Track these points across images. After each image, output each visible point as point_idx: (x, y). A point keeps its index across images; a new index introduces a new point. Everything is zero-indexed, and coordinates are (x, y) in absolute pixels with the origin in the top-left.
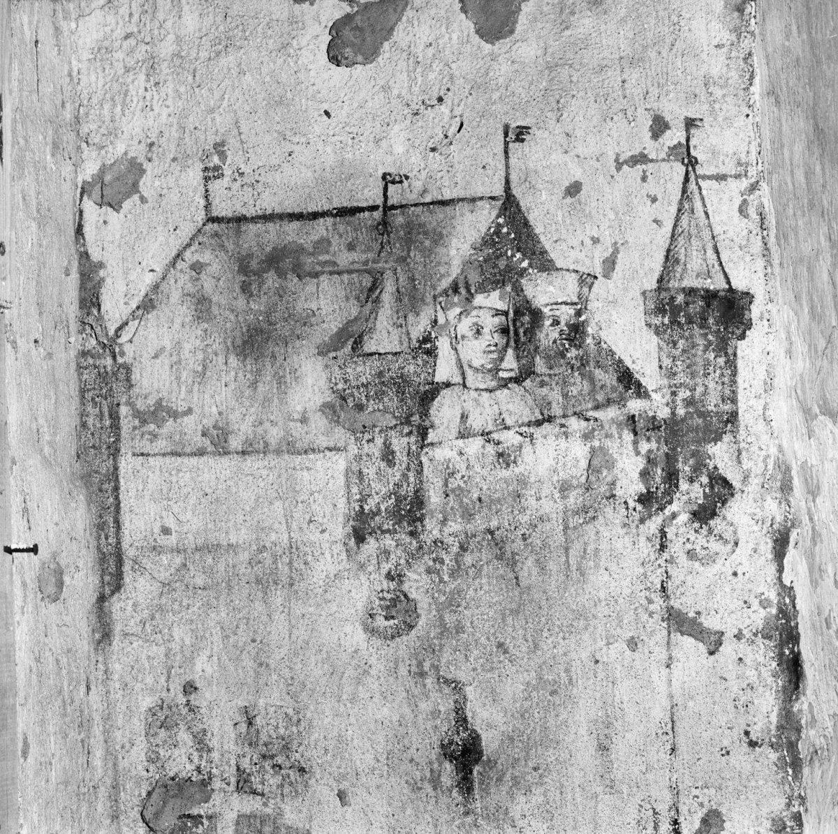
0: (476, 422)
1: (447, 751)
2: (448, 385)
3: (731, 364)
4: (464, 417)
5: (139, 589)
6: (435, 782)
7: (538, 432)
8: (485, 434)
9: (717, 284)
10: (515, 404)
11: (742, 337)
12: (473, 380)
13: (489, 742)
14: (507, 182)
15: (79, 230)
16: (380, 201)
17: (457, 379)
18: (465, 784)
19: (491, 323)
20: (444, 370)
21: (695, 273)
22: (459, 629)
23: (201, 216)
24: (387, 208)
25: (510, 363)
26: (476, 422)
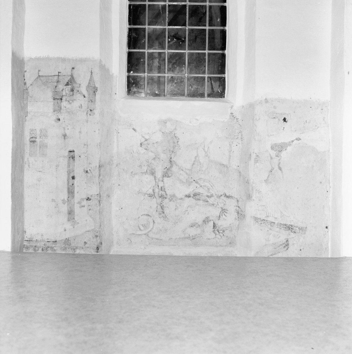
0: (67, 100)
2: (65, 95)
8: (68, 101)
13: (68, 134)
17: (66, 95)
18: (65, 138)
19: (69, 89)
23: (38, 76)
24: (59, 76)
26: (67, 100)
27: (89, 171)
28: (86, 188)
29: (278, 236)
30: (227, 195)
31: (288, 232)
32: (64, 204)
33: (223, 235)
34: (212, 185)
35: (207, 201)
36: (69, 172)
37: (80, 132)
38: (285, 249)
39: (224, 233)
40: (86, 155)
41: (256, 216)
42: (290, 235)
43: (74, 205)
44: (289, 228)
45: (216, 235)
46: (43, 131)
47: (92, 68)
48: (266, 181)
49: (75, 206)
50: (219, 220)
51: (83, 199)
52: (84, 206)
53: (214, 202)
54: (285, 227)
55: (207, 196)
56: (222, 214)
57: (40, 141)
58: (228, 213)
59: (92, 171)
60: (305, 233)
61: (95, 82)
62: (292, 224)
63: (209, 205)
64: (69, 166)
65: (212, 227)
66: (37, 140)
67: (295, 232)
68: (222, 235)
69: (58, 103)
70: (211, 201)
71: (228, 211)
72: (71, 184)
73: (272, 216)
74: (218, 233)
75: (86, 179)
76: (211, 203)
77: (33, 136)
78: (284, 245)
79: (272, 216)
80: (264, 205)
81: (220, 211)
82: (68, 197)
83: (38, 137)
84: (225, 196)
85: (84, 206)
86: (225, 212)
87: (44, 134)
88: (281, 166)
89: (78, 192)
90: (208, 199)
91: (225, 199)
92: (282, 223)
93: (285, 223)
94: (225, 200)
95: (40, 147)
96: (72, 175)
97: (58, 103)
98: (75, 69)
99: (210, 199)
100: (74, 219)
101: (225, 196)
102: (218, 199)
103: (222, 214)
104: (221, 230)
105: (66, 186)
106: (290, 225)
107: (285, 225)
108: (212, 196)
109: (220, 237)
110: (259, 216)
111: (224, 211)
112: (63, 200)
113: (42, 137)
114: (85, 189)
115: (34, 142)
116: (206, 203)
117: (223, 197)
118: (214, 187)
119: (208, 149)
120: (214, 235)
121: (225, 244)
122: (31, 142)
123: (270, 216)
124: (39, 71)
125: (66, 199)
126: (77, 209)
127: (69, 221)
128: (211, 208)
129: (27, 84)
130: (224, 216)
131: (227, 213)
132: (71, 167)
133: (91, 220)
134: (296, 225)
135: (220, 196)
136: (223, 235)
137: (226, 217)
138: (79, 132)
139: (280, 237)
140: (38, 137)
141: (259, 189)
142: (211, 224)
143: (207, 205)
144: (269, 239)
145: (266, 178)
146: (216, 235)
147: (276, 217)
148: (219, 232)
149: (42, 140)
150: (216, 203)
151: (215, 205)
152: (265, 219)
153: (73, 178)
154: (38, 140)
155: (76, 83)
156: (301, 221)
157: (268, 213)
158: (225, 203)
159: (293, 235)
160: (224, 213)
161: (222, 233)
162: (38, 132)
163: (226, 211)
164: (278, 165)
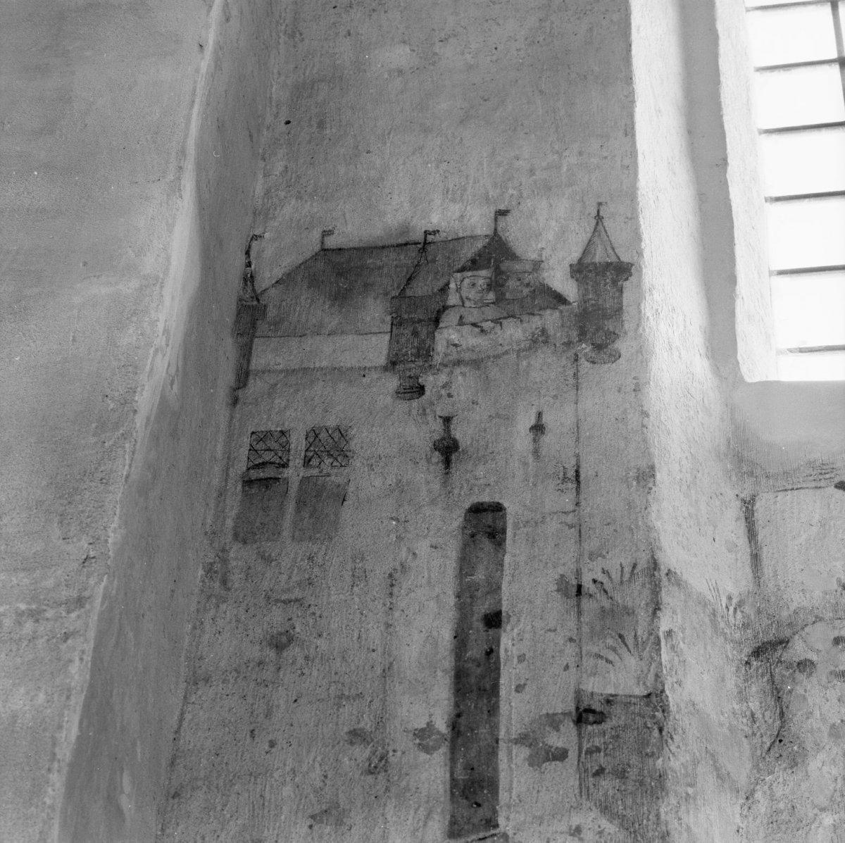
1: (436, 447)
3: (621, 291)
4: (461, 317)
5: (256, 386)
6: (429, 461)
7: (505, 322)
9: (613, 259)
10: (491, 312)
11: (627, 279)
12: (467, 304)
13: (462, 445)
14: (496, 229)
15: (248, 253)
16: (422, 240)
18: (447, 463)
19: (481, 282)
20: (453, 299)
21: (599, 256)
22: (450, 396)
25: (491, 296)
27: (586, 582)
28: (572, 665)
32: (427, 749)
36: (466, 595)
37: (538, 428)
40: (570, 519)
43: (493, 752)
46: (323, 435)
47: (600, 204)
49: (502, 755)
51: (553, 721)
52: (561, 755)
57: (305, 480)
59: (608, 586)
61: (615, 245)
64: (465, 565)
66: (288, 473)
69: (415, 334)
72: (475, 651)
75: (572, 624)
77: (267, 457)
82: (459, 716)
83: (296, 462)
85: (561, 755)
87: (331, 445)
89: (519, 688)
95: (301, 504)
96: (483, 607)
97: (415, 334)
98: (515, 213)
100: (491, 823)
105: (448, 663)
112: (423, 736)
113: (315, 462)
114: (567, 667)
115: (267, 482)
122: (248, 483)
124: (326, 233)
125: (442, 725)
126: (514, 773)
127: (459, 835)
129: (258, 279)
132: (480, 576)
133: (610, 828)
138: (532, 428)
140: (296, 462)
149: (315, 472)
153: (494, 620)
154: (294, 473)
155: (513, 257)
162: (298, 442)
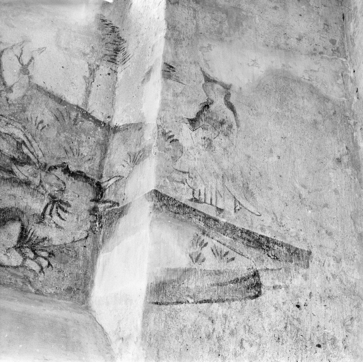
29: (229, 256)
30: (73, 169)
31: (256, 252)
33: (49, 264)
34: (30, 137)
35: (11, 172)
38: (252, 293)
39: (51, 260)
41: (163, 191)
42: (263, 261)
44: (260, 243)
45: (25, 259)
48: (193, 122)
50: (39, 223)
53: (31, 178)
54: (248, 237)
55: (13, 159)
56: (51, 210)
58: (70, 211)
60: (308, 266)
62: (268, 234)
63: (15, 181)
65: (15, 238)
67: (276, 258)
68: (45, 263)
70: (23, 172)
71: (70, 206)
73: (208, 201)
74: (32, 255)
76: (22, 177)
78: (247, 283)
79: (208, 201)
80: (187, 171)
81: (46, 201)
84: (66, 170)
86: (61, 208)
88: (232, 100)
90: (15, 168)
91: (63, 177)
92: (238, 225)
93: (247, 228)
94: (65, 181)
99: (20, 168)
101: (66, 170)
102: (43, 174)
103: (51, 210)
104: (43, 250)
106: (263, 236)
107: (248, 233)
108: (27, 161)
109: (37, 268)
110: (172, 194)
111: (57, 203)
116: (6, 176)
117: (59, 172)
118: (35, 144)
119: (30, 61)
120: (20, 259)
121: (50, 290)
123: (205, 202)
128: (18, 191)
130: (56, 218)
131: (66, 212)
134: (279, 239)
135: (50, 169)
136: (49, 264)
137: (63, 222)
139: (233, 259)
141: (171, 134)
142: (15, 229)
143: (7, 179)
144: (201, 258)
145: (193, 116)
146: (25, 259)
147: (220, 206)
148: (35, 254)
150: (37, 182)
151: (32, 187)
152: (190, 204)
156: (294, 234)
157: (196, 193)
158: (63, 187)
159: (270, 264)
160: (60, 211)
161: (45, 259)
163: (64, 206)
164: (225, 98)
